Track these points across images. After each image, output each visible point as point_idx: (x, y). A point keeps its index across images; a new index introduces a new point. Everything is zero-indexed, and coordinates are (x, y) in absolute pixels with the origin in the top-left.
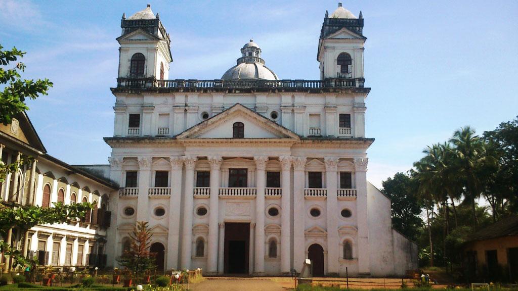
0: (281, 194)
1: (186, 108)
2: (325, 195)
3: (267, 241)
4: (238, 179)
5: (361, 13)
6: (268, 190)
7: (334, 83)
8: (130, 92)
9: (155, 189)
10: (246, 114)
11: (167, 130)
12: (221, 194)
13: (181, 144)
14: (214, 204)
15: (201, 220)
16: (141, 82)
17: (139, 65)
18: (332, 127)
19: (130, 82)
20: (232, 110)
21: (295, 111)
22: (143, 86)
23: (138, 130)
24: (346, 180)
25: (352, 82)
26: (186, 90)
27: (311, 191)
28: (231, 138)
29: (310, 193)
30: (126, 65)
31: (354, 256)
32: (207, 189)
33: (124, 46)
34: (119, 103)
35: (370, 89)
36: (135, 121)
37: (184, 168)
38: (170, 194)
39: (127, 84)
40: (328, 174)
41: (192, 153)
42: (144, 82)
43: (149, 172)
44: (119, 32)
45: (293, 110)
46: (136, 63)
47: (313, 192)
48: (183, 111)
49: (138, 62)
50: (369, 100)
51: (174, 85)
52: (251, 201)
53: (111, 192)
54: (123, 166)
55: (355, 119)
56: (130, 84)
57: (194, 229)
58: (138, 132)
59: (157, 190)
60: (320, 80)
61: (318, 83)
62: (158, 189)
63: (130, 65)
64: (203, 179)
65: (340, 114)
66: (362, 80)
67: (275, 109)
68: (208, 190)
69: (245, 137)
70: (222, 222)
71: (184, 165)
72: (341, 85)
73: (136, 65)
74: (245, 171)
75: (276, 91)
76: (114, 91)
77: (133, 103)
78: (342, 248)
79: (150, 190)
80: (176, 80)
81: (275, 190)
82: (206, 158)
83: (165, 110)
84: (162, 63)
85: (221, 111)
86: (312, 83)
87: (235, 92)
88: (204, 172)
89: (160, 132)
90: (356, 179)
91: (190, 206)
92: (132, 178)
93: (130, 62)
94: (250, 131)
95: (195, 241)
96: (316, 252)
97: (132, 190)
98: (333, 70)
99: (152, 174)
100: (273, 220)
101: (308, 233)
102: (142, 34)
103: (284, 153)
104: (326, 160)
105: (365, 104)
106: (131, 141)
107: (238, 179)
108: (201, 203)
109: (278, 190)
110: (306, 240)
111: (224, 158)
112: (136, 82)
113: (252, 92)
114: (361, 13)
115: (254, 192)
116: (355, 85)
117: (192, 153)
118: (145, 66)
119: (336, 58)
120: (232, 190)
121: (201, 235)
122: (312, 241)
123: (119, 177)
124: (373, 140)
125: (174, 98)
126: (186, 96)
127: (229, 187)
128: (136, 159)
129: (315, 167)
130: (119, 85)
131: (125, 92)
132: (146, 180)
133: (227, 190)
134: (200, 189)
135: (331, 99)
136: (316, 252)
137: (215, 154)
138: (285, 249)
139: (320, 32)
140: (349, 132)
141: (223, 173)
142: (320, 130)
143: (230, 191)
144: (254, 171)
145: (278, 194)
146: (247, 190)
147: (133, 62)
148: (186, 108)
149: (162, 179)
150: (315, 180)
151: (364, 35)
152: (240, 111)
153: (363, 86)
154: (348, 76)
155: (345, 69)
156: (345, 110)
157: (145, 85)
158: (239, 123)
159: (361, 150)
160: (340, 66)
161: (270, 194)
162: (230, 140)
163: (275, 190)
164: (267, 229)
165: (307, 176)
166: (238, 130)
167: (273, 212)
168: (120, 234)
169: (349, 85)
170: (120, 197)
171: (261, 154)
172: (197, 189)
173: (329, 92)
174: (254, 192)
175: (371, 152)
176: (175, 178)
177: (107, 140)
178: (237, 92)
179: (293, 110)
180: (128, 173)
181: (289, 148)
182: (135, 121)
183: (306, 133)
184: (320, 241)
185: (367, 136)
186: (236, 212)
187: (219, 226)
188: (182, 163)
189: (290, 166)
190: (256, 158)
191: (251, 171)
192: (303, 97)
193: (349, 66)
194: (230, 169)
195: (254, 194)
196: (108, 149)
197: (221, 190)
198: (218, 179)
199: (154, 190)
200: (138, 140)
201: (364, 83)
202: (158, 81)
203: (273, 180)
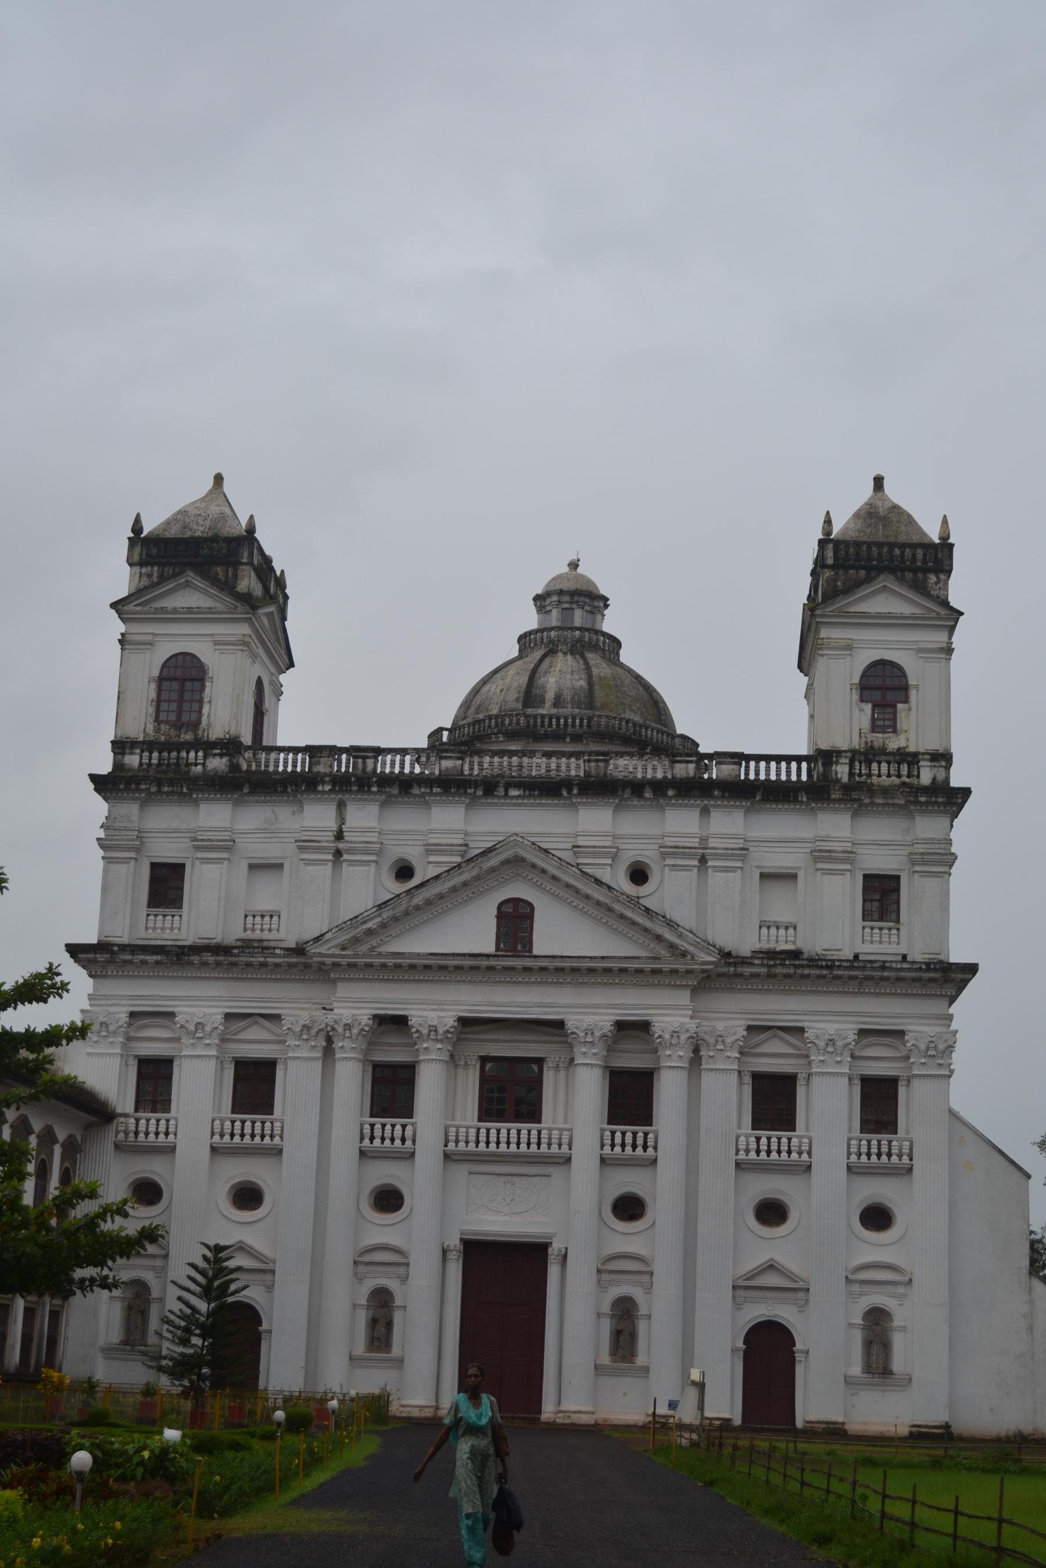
0: (655, 1148)
1: (341, 845)
3: (606, 1308)
4: (511, 1093)
5: (945, 521)
6: (613, 1133)
7: (846, 769)
8: (154, 789)
9: (233, 1122)
10: (544, 871)
11: (275, 919)
12: (451, 1146)
13: (320, 969)
14: (421, 1179)
15: (384, 1229)
16: (192, 754)
17: (187, 696)
19: (155, 754)
20: (493, 861)
21: (710, 863)
22: (199, 768)
23: (177, 918)
24: (879, 1103)
25: (909, 764)
26: (342, 784)
27: (758, 1139)
28: (488, 956)
29: (753, 1145)
30: (145, 692)
31: (897, 1365)
32: (404, 1127)
33: (135, 628)
34: (117, 825)
36: (166, 885)
37: (329, 1051)
38: (281, 1137)
39: (145, 761)
40: (815, 1081)
42: (201, 754)
43: (209, 1067)
44: (120, 580)
45: (703, 860)
46: (175, 685)
47: (764, 1141)
48: (330, 857)
49: (183, 679)
50: (966, 831)
51: (301, 764)
52: (556, 1172)
53: (88, 1127)
54: (129, 1039)
55: (912, 893)
56: (154, 761)
57: (363, 1260)
58: (176, 925)
59: (238, 1124)
60: (803, 750)
61: (804, 765)
62: (243, 1122)
63: (153, 695)
64: (392, 1091)
65: (865, 876)
66: (943, 758)
67: (648, 854)
68: (409, 1130)
69: (535, 952)
70: (454, 1241)
71: (329, 1040)
72: (870, 775)
73: (174, 696)
74: (535, 1068)
75: (648, 794)
76: (100, 783)
78: (858, 1337)
79: (217, 1122)
81: (635, 1134)
83: (270, 852)
84: (259, 682)
85: (458, 859)
86: (783, 764)
87: (506, 794)
88: (395, 1067)
89: (249, 926)
90: (913, 1105)
91: (348, 1181)
92: (155, 1079)
93: (153, 686)
94: (558, 932)
95: (363, 1301)
96: (769, 1353)
97: (158, 1121)
98: (850, 725)
99: (222, 1069)
100: (626, 1238)
101: (744, 1288)
102: (197, 589)
104: (809, 1035)
105: (949, 842)
106: (155, 958)
107: (511, 1093)
109: (646, 1134)
110: (737, 1304)
111: (465, 1022)
112: (174, 754)
113: (565, 793)
114: (945, 521)
115: (565, 1141)
116: (918, 776)
118: (206, 700)
119: (856, 680)
120: (488, 1130)
121: (383, 1282)
122: (758, 1311)
124: (972, 969)
125: (302, 808)
126: (341, 806)
127: (480, 1120)
128: (172, 1015)
129: (776, 1057)
130: (118, 766)
131: (138, 789)
133: (473, 1132)
134: (384, 1126)
135: (834, 826)
136: (769, 1353)
138: (657, 1338)
139: (808, 580)
140: (894, 939)
141: (460, 1071)
142: (795, 928)
143: (483, 1131)
144: (567, 1068)
145: (645, 1147)
146: (539, 1132)
147: (166, 685)
148: (341, 845)
149: (254, 1085)
150: (774, 1101)
151: (954, 602)
152: (523, 860)
153: (947, 778)
154: (894, 743)
155: (885, 717)
156: (882, 862)
157: (204, 765)
158: (516, 901)
159: (935, 1006)
160: (868, 708)
161: (618, 1149)
162: (485, 963)
163: (635, 1134)
164: (607, 1269)
165: (748, 1090)
166: (515, 922)
167: (629, 1208)
169: (899, 776)
170: (117, 1146)
171: (591, 1012)
172: (372, 1126)
173: (829, 800)
174: (565, 1141)
176: (296, 1085)
178: (514, 792)
179: (703, 860)
181: (687, 994)
182: (166, 885)
183: (745, 939)
184: (784, 1313)
185: (956, 957)
187: (444, 1252)
188: (322, 1037)
189: (684, 1053)
190: (572, 1022)
191: (557, 1068)
192: (739, 816)
193: (899, 706)
194: (484, 1060)
195: (565, 1148)
197: (452, 1131)
199: (228, 1124)
200: (180, 958)
201: (948, 768)
202: (248, 748)
203: (630, 1098)
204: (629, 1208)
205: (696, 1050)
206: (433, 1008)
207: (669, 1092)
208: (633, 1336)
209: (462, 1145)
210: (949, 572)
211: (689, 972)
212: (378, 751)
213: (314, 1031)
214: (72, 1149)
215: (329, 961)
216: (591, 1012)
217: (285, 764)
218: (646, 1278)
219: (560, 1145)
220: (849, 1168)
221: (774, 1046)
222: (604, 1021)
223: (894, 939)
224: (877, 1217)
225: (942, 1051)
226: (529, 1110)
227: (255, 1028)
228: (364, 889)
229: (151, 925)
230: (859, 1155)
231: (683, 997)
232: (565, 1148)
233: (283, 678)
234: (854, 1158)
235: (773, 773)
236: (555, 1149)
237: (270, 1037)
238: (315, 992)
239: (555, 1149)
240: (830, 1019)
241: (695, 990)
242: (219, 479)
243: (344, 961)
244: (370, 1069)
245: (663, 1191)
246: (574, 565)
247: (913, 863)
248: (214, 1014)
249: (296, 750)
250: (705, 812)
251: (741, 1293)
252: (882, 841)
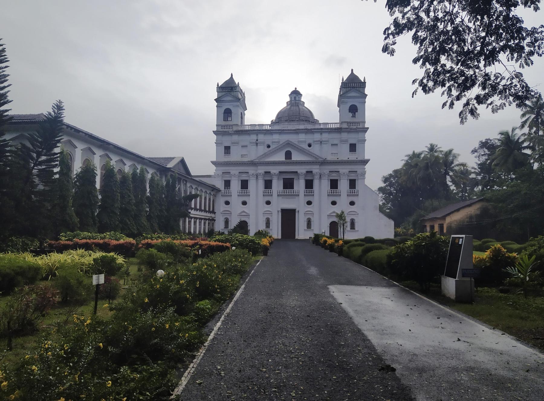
4: (288, 184)
14: (274, 199)
15: (268, 208)
18: (345, 154)
24: (353, 184)
35: (368, 128)
36: (227, 149)
37: (257, 178)
41: (261, 170)
43: (237, 181)
45: (321, 142)
50: (367, 135)
52: (297, 197)
64: (268, 185)
66: (364, 122)
67: (311, 141)
70: (280, 210)
77: (227, 141)
80: (251, 125)
82: (270, 172)
90: (358, 184)
92: (227, 184)
94: (296, 157)
100: (309, 208)
101: (329, 216)
103: (316, 169)
107: (288, 184)
108: (268, 198)
111: (280, 172)
117: (261, 170)
123: (220, 185)
129: (334, 177)
132: (235, 186)
135: (344, 135)
137: (275, 170)
139: (339, 90)
149: (244, 185)
150: (334, 184)
151: (366, 93)
155: (354, 116)
159: (362, 167)
166: (288, 155)
168: (223, 216)
175: (367, 167)
176: (252, 185)
177: (213, 163)
179: (321, 142)
180: (225, 181)
182: (227, 149)
186: (288, 204)
189: (318, 176)
190: (299, 171)
196: (214, 168)
198: (277, 185)
203: (309, 185)
204: (309, 203)
206: (275, 170)
207: (316, 183)
208: (311, 224)
210: (365, 87)
212: (263, 125)
214: (215, 196)
216: (301, 170)
217: (247, 128)
221: (334, 174)
222: (304, 171)
225: (363, 174)
226: (292, 187)
228: (262, 150)
231: (318, 167)
235: (334, 126)
240: (344, 170)
242: (232, 75)
245: (315, 200)
246: (296, 88)
248: (237, 173)
249: (248, 125)
250: (321, 134)
252: (352, 138)
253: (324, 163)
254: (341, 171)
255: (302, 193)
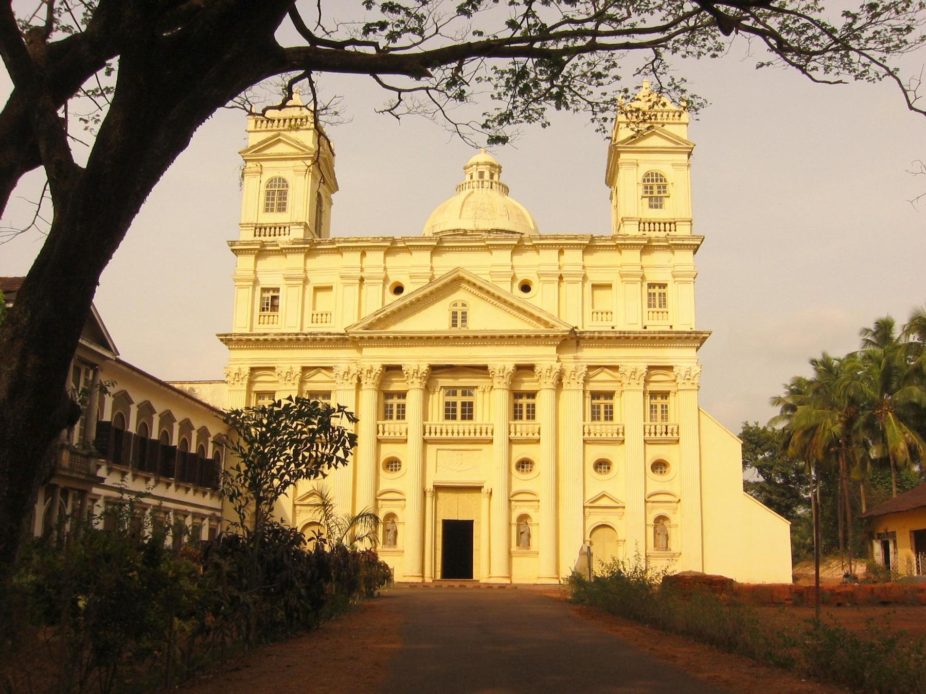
2: (621, 435)
12: (427, 435)
41: (375, 358)
45: (561, 277)
67: (532, 276)
70: (429, 487)
71: (359, 380)
103: (544, 357)
115: (489, 431)
117: (375, 358)
148: (363, 275)
171: (501, 359)
179: (561, 277)
188: (355, 378)
195: (489, 435)
205: (560, 380)
206: (415, 359)
209: (433, 435)
211: (555, 337)
213: (350, 376)
215: (357, 336)
216: (501, 359)
218: (536, 503)
219: (487, 433)
220: (645, 441)
221: (604, 376)
223: (665, 317)
224: (659, 466)
227: (319, 374)
229: (262, 321)
230: (650, 433)
232: (489, 435)
233: (333, 196)
234: (647, 435)
236: (484, 435)
237: (328, 379)
238: (352, 353)
239: (484, 435)
241: (559, 349)
243: (366, 336)
244: (382, 395)
245: (540, 454)
247: (674, 277)
251: (587, 510)
253: (573, 340)
254: (627, 366)
255: (500, 438)
